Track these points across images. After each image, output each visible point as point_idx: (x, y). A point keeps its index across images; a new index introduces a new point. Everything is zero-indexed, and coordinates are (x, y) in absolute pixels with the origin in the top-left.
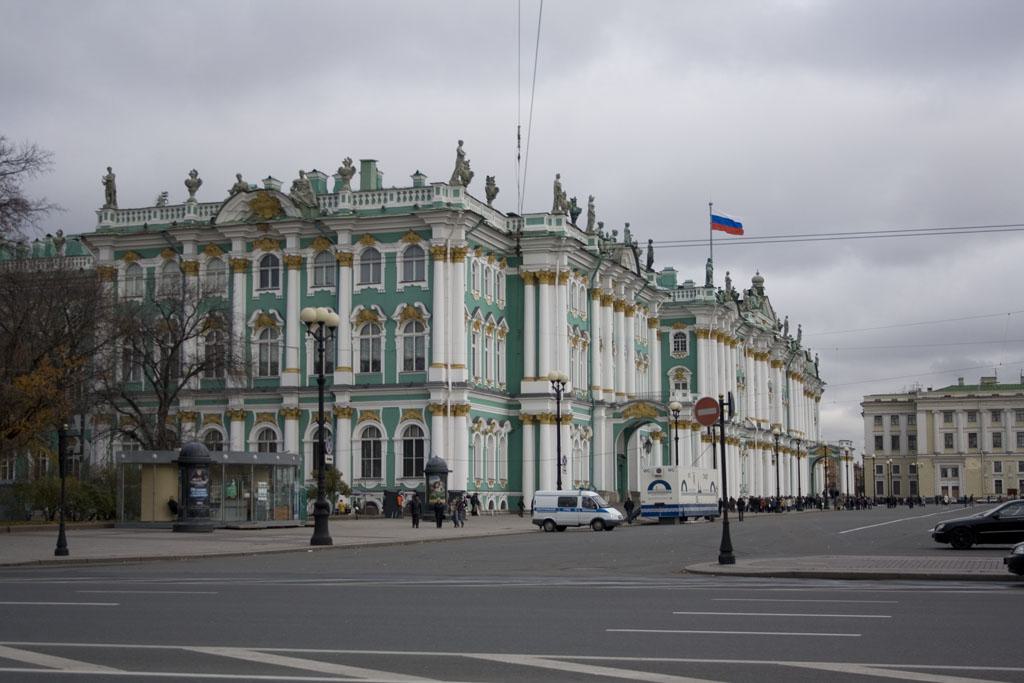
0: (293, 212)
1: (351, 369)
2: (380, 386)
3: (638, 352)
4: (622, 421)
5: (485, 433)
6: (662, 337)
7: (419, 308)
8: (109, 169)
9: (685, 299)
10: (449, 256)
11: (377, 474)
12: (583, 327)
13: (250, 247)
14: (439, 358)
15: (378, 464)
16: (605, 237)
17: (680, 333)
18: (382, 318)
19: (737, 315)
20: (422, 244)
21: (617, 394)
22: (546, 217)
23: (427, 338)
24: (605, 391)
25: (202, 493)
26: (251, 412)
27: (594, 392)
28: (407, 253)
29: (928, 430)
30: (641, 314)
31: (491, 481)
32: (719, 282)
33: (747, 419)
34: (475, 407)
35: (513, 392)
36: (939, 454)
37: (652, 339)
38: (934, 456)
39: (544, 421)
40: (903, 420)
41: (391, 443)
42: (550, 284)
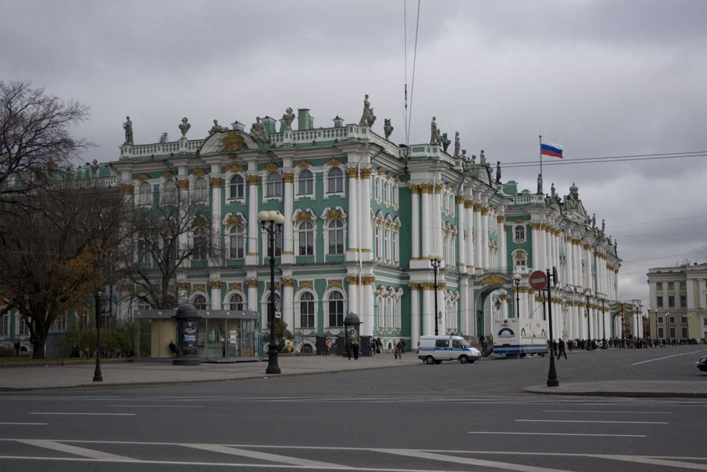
0: (252, 146)
1: (293, 253)
2: (314, 264)
3: (491, 240)
4: (480, 287)
6: (508, 229)
7: (339, 211)
8: (128, 118)
9: (523, 203)
10: (359, 175)
11: (312, 325)
12: (452, 222)
13: (223, 170)
14: (354, 245)
15: (312, 318)
17: (520, 226)
18: (314, 218)
19: (559, 214)
20: (341, 166)
21: (476, 269)
22: (426, 147)
23: (345, 231)
24: (468, 267)
25: (192, 338)
26: (225, 283)
27: (461, 267)
30: (493, 213)
31: (390, 329)
32: (546, 190)
33: (567, 285)
34: (378, 278)
35: (404, 268)
37: (500, 230)
39: (425, 287)
40: (677, 285)
41: (321, 303)
42: (429, 193)
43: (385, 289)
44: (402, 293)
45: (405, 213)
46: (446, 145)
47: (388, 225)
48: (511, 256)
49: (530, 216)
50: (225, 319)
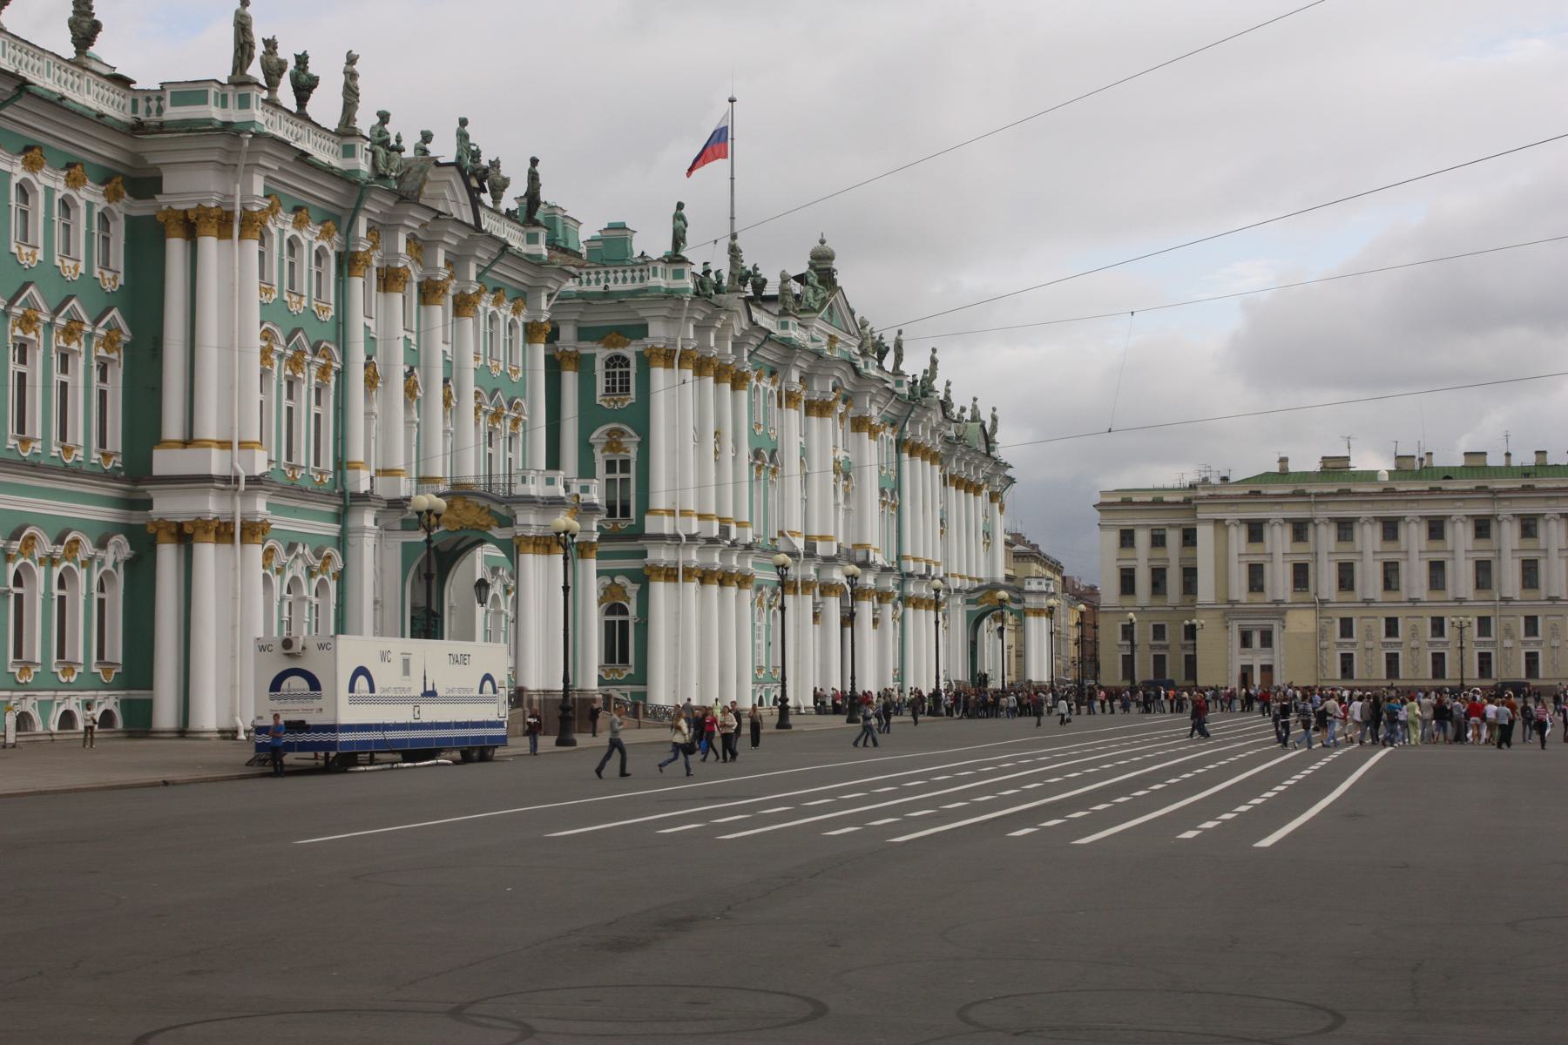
9: (629, 286)
12: (328, 333)
16: (393, 142)
17: (617, 357)
19: (745, 324)
22: (213, 90)
27: (350, 473)
29: (1218, 559)
33: (781, 533)
35: (135, 475)
36: (1237, 602)
38: (1229, 609)
39: (199, 534)
40: (1174, 538)
42: (220, 237)
44: (126, 551)
45: (142, 300)
47: (69, 333)
48: (592, 446)
49: (646, 326)
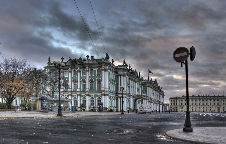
0: (79, 63)
1: (89, 88)
2: (94, 91)
3: (137, 88)
4: (135, 98)
5: (112, 99)
6: (141, 87)
7: (100, 79)
11: (93, 105)
12: (129, 84)
13: (72, 69)
14: (103, 87)
15: (93, 103)
18: (94, 80)
20: (101, 69)
21: (134, 94)
23: (101, 83)
24: (132, 94)
25: (45, 105)
26: (72, 95)
27: (130, 94)
28: (98, 70)
30: (138, 83)
31: (113, 107)
32: (150, 79)
34: (110, 95)
35: (116, 93)
37: (140, 87)
38: (180, 106)
40: (175, 101)
41: (95, 100)
43: (112, 98)
44: (116, 99)
46: (127, 66)
47: (112, 83)
50: (53, 100)
